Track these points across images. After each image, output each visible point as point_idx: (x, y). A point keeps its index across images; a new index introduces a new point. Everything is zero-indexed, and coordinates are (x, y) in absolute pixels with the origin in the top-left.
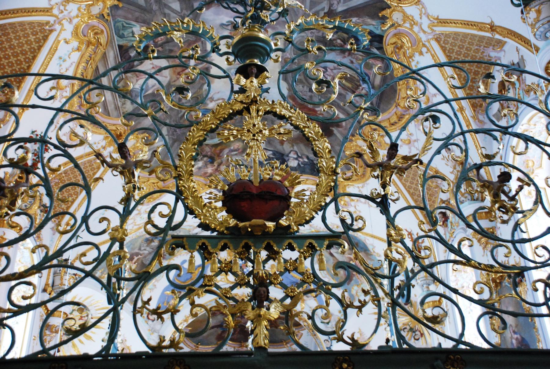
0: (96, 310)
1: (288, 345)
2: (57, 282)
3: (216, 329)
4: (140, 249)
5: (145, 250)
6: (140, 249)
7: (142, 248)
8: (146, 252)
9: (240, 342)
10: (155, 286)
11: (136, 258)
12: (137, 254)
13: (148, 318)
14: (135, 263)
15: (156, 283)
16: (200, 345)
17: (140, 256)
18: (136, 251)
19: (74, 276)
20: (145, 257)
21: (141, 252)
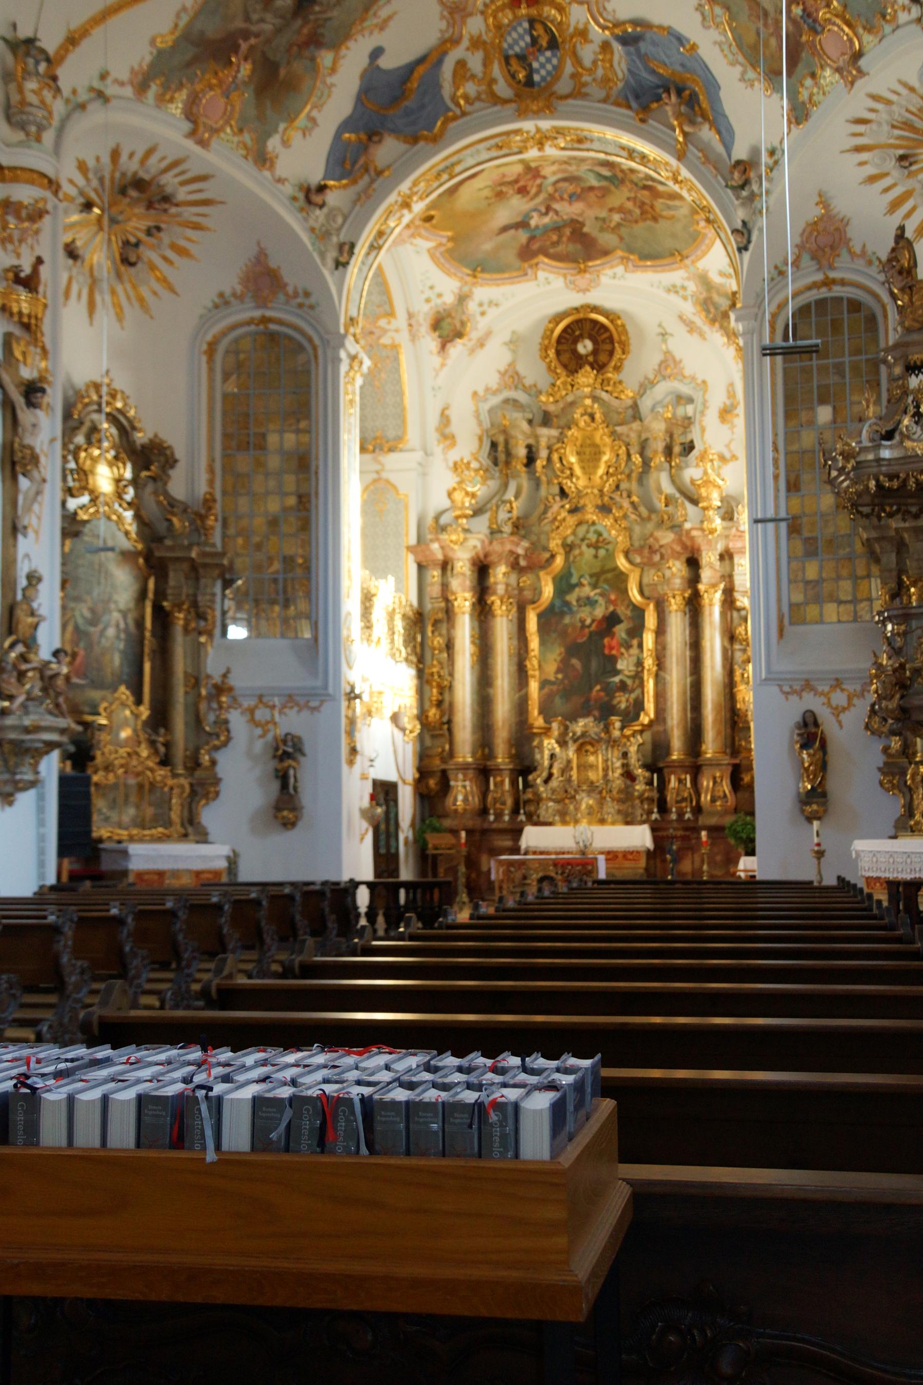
0: (183, 183)
1: (687, 262)
2: (15, 98)
3: (512, 232)
4: (247, 19)
5: (262, 20)
6: (247, 19)
7: (255, 17)
8: (267, 27)
9: (575, 261)
10: (313, 121)
11: (244, 46)
12: (246, 34)
13: (309, 201)
14: (246, 59)
15: (314, 113)
16: (483, 271)
17: (253, 41)
18: (239, 24)
19: (51, 83)
20: (268, 41)
21: (254, 28)
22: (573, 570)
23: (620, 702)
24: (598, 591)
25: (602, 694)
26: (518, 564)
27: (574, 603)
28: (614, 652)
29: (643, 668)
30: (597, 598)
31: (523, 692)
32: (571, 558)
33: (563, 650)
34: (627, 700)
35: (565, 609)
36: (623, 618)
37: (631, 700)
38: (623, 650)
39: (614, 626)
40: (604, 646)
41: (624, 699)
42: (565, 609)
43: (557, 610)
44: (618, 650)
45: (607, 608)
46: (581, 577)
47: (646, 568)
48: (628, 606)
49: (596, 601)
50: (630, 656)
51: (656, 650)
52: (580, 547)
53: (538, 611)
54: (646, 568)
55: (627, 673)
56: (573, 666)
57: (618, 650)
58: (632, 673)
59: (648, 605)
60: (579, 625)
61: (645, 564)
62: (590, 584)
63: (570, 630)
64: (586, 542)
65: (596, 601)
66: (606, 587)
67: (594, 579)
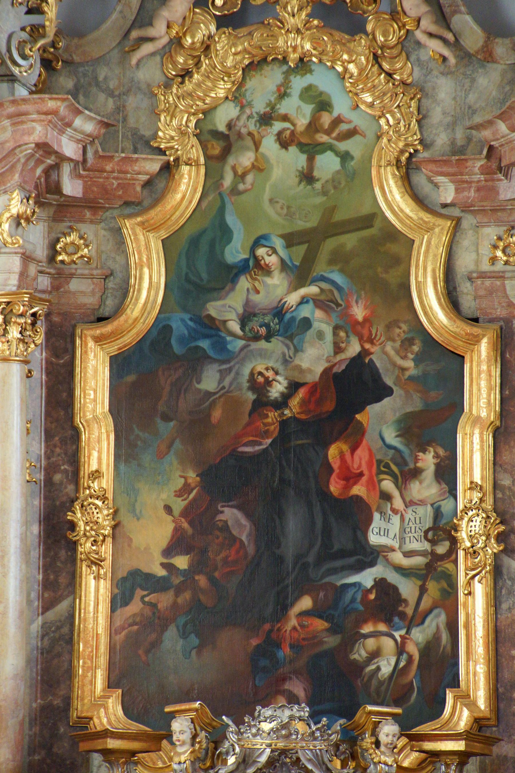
22: (231, 219)
23: (376, 654)
24: (313, 290)
25: (321, 625)
26: (57, 189)
27: (235, 326)
28: (358, 490)
29: (454, 542)
30: (306, 311)
31: (63, 606)
32: (228, 180)
33: (192, 476)
34: (401, 650)
35: (205, 344)
36: (389, 381)
37: (412, 649)
38: (388, 485)
39: (361, 409)
40: (330, 469)
41: (388, 644)
42: (205, 344)
43: (177, 348)
44: (372, 485)
45: (338, 349)
46: (257, 243)
47: (468, 221)
48: (408, 342)
49: (307, 323)
50: (409, 504)
51: (496, 486)
52: (257, 145)
53: (114, 348)
54: (468, 221)
55: (398, 558)
56: (225, 528)
57: (372, 485)
58: (419, 561)
59: (476, 340)
60: (251, 396)
61: (467, 208)
62: (284, 266)
63: (217, 414)
64: (278, 126)
65: (307, 323)
66: (338, 278)
67: (301, 250)
